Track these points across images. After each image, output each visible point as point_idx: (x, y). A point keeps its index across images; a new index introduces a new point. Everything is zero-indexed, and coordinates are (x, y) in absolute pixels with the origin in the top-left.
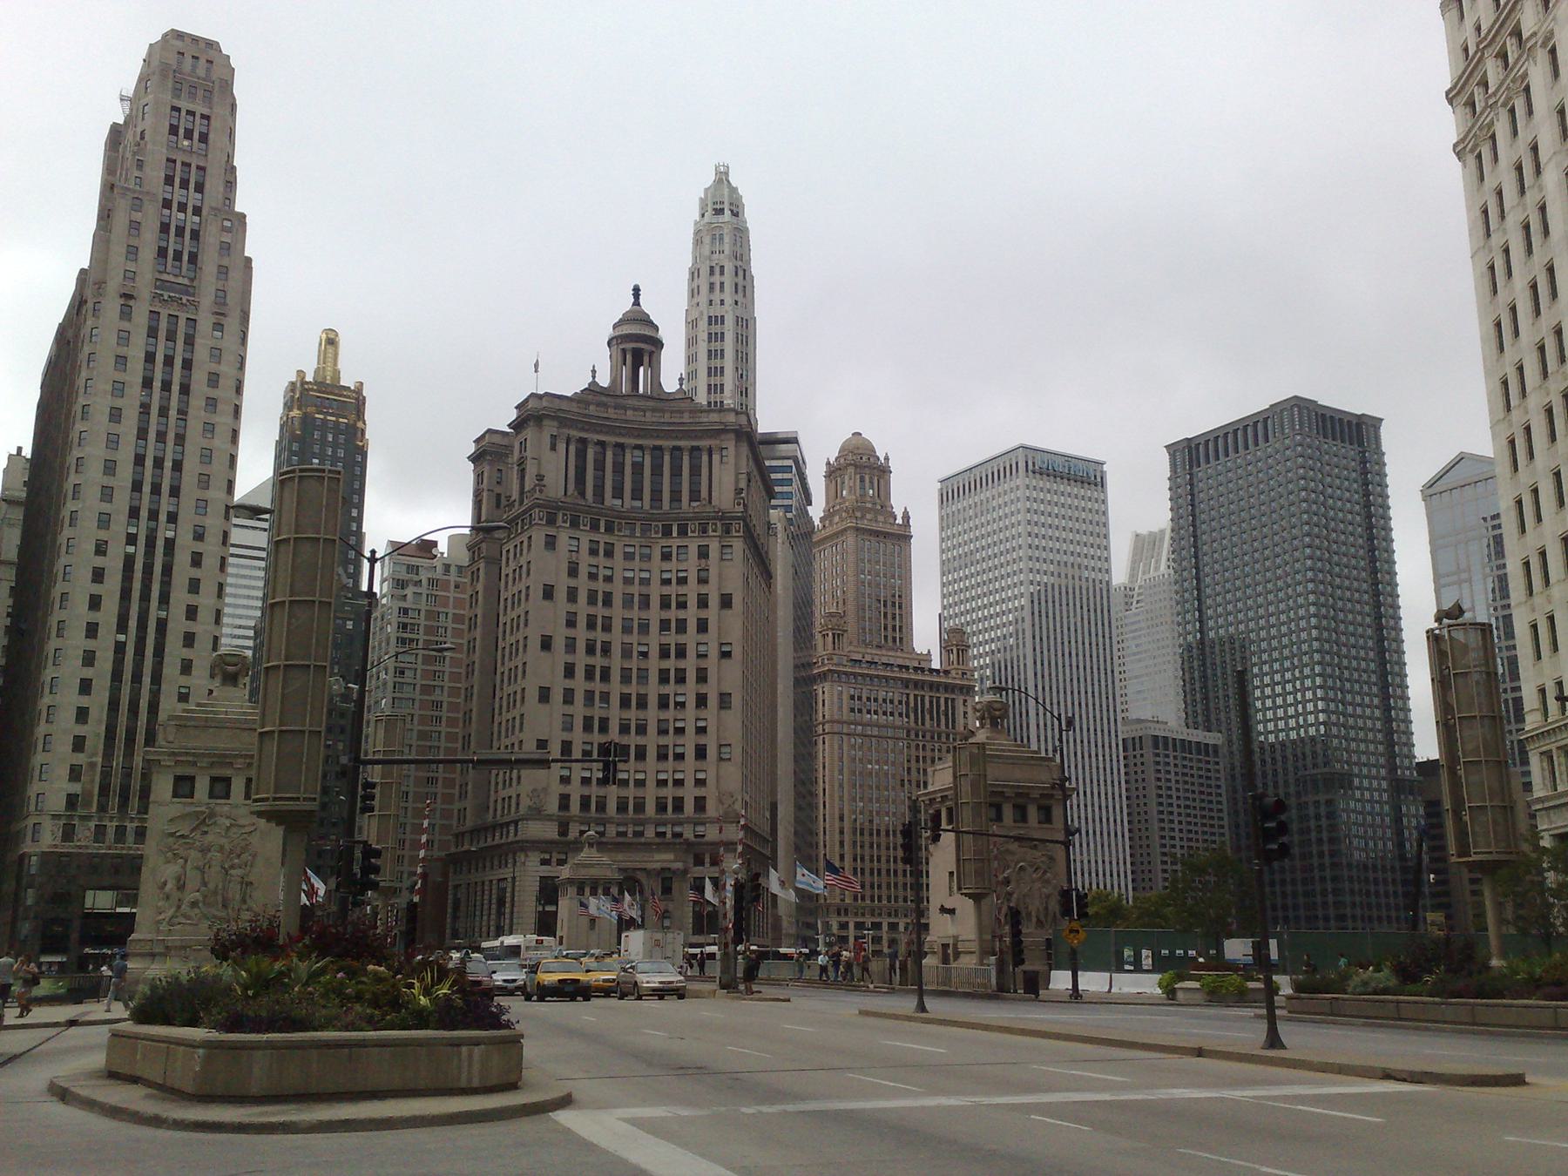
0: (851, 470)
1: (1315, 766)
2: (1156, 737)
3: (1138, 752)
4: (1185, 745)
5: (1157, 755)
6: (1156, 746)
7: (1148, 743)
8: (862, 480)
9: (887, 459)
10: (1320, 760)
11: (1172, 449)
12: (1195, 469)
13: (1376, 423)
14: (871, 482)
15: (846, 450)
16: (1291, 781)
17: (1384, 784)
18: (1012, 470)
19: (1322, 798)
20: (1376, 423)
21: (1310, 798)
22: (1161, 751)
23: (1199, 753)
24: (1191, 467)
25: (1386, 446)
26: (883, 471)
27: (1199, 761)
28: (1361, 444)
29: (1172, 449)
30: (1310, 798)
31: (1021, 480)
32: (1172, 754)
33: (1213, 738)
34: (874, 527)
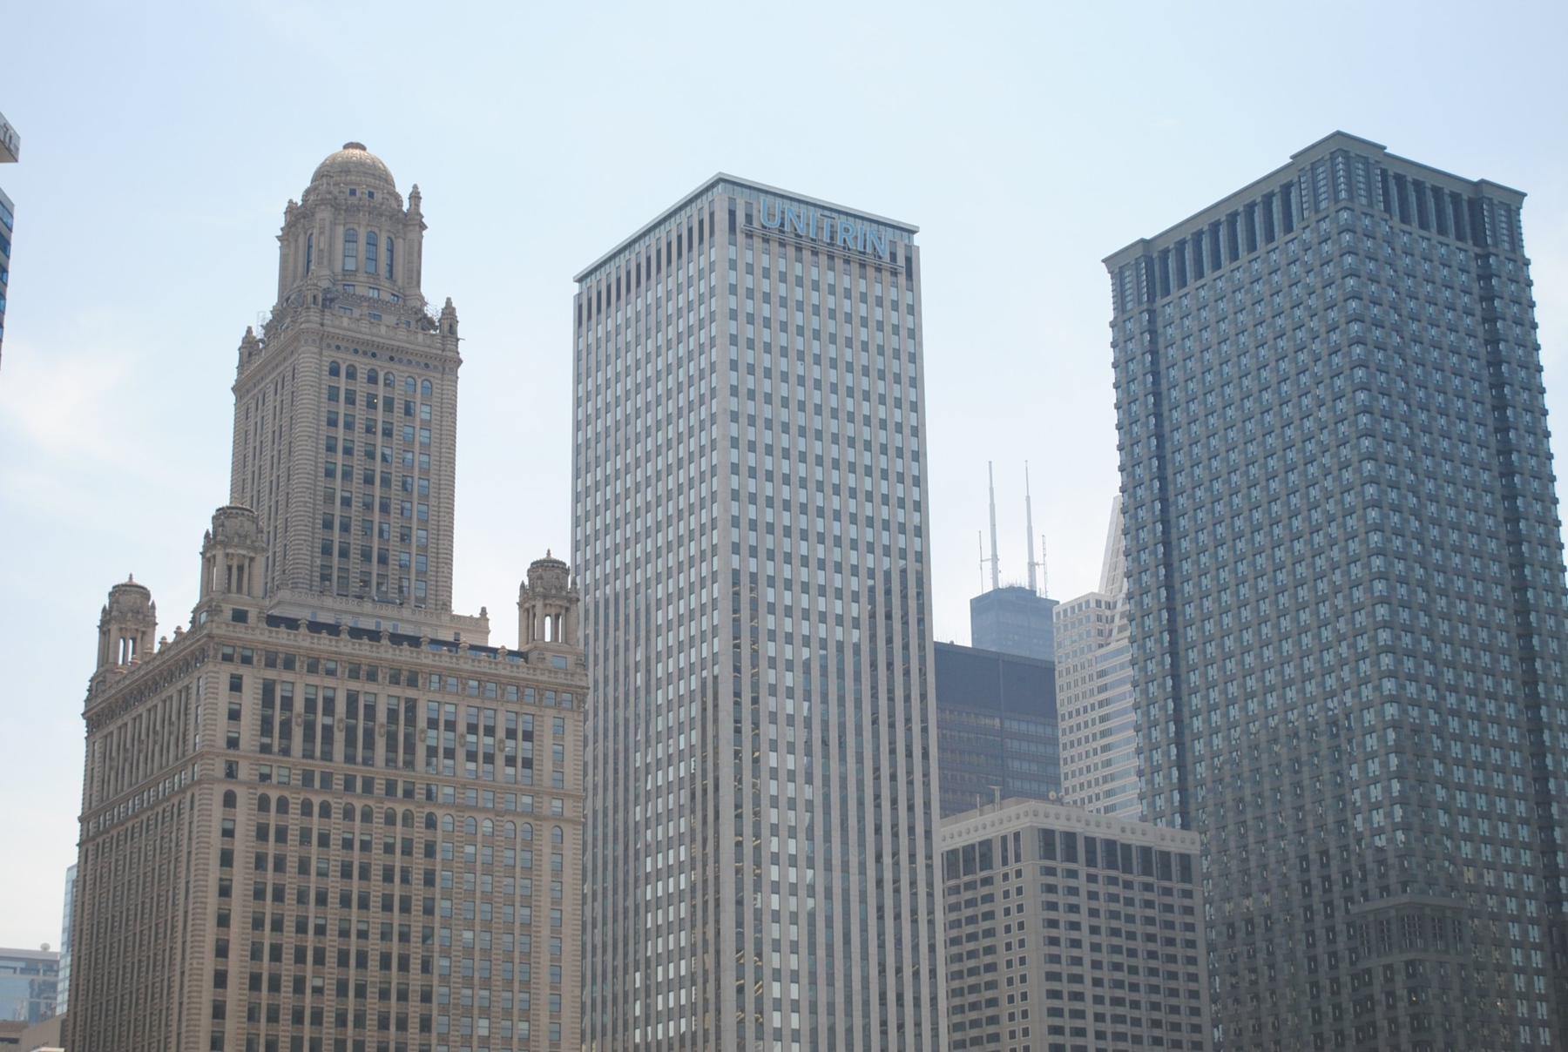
0: (324, 214)
1: (1385, 889)
2: (1047, 836)
3: (1013, 867)
4: (1115, 854)
5: (1050, 872)
6: (1049, 853)
7: (1030, 846)
8: (350, 238)
9: (415, 197)
10: (1393, 878)
11: (1117, 265)
12: (1159, 302)
13: (1512, 201)
14: (372, 242)
15: (322, 174)
16: (1340, 927)
17: (1535, 934)
18: (700, 233)
19: (1398, 959)
20: (1512, 201)
21: (1375, 963)
22: (1060, 865)
23: (1147, 871)
24: (1151, 300)
25: (1528, 252)
26: (410, 223)
27: (1148, 887)
28: (1479, 240)
29: (1117, 265)
30: (1375, 963)
31: (719, 250)
32: (1083, 869)
33: (1172, 839)
34: (365, 331)
